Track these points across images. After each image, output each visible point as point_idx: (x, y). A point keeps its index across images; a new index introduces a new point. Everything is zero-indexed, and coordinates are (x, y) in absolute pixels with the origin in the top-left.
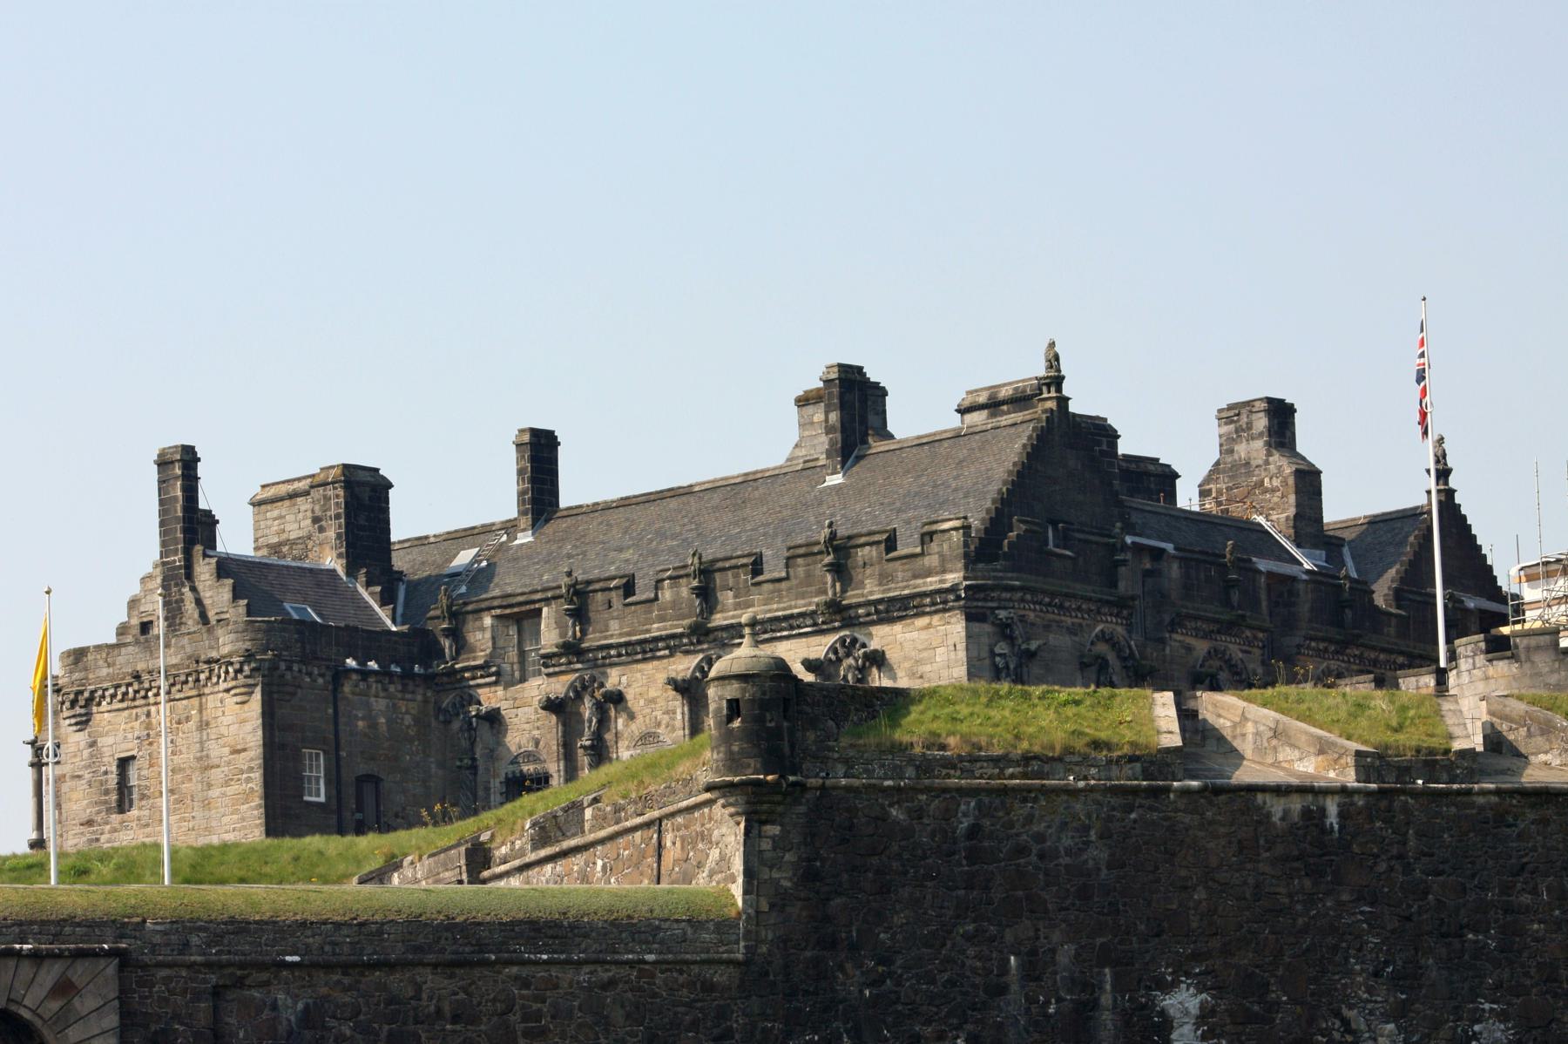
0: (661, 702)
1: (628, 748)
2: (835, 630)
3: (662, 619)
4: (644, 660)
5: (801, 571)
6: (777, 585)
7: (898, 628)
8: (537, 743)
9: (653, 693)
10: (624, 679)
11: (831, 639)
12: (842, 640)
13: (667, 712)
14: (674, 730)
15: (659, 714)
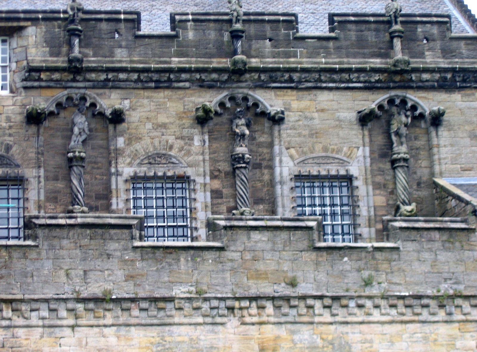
0: (173, 129)
1: (130, 164)
2: (388, 88)
3: (179, 55)
4: (156, 88)
5: (353, 35)
6: (324, 43)
7: (457, 97)
8: (8, 148)
9: (162, 119)
10: (127, 103)
11: (381, 97)
12: (391, 101)
13: (182, 138)
14: (189, 153)
15: (171, 140)
